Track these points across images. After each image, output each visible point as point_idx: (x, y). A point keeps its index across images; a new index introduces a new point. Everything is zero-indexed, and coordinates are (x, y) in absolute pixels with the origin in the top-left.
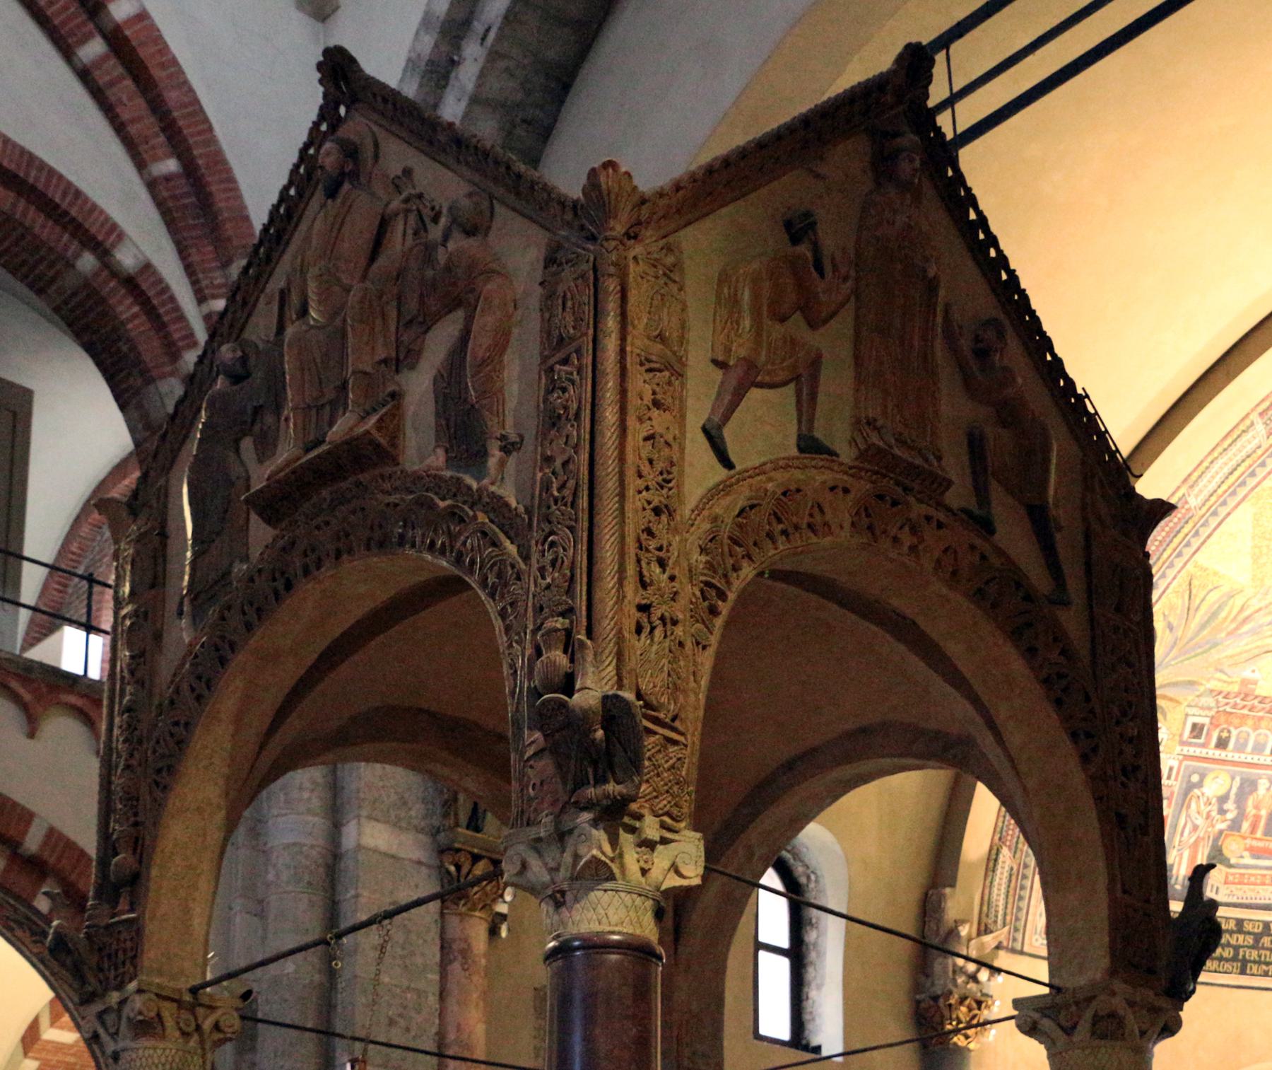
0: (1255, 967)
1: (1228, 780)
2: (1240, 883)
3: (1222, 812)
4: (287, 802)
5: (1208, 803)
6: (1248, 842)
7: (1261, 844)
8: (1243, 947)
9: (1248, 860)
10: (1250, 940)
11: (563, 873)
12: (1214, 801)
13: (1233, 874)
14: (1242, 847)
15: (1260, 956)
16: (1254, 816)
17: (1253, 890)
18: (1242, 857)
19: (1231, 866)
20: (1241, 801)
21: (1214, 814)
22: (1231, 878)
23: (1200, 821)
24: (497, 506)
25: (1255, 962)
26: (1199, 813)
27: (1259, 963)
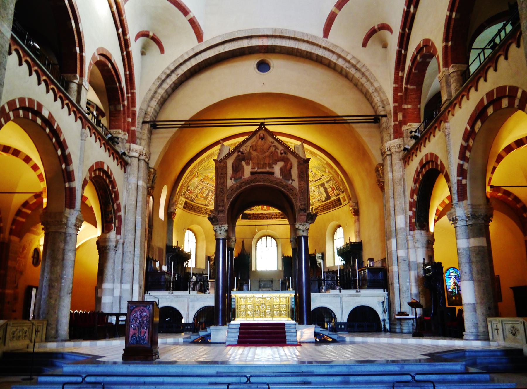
4: (134, 176)
9: (199, 197)
11: (304, 229)
23: (197, 191)
24: (293, 187)
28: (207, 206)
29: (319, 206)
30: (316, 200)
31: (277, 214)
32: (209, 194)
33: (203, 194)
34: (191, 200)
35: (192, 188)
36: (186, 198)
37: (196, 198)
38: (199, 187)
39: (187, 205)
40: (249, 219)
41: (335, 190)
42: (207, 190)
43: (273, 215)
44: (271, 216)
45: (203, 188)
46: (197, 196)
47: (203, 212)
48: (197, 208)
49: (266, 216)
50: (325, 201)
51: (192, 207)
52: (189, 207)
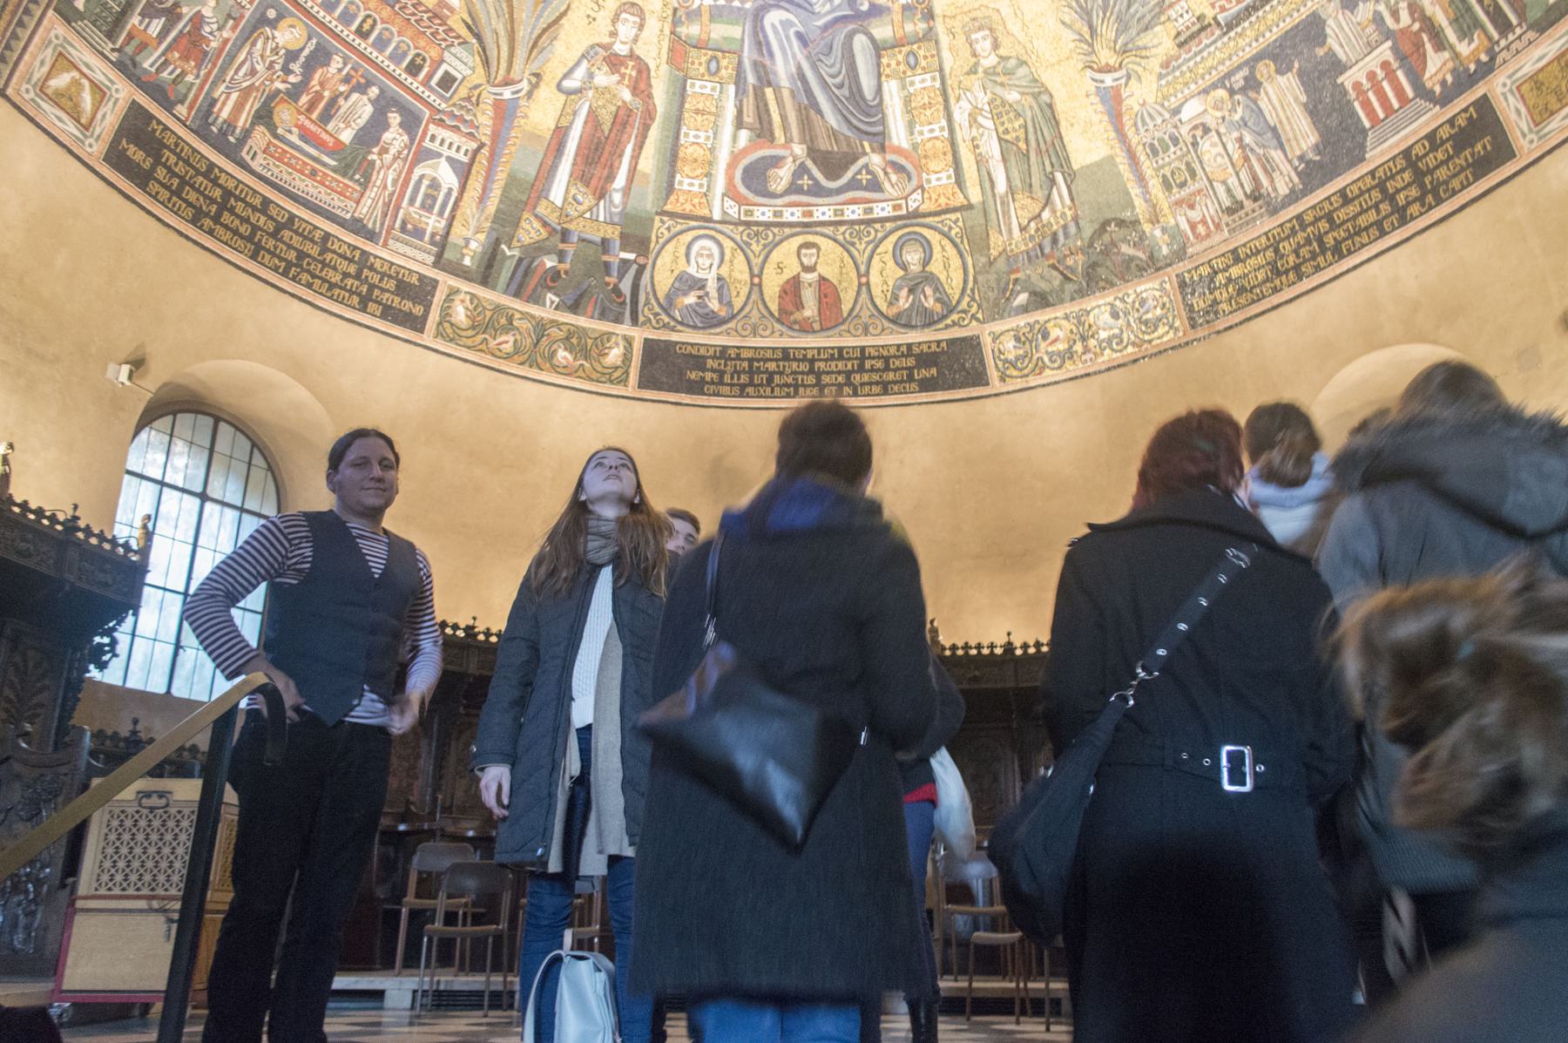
0: (268, 257)
1: (305, 35)
2: (278, 159)
3: (287, 70)
5: (275, 51)
6: (302, 118)
7: (313, 128)
8: (261, 229)
10: (271, 227)
12: (282, 52)
13: (275, 146)
14: (294, 122)
15: (276, 248)
16: (316, 92)
17: (290, 174)
18: (290, 132)
19: (276, 136)
20: (309, 69)
21: (278, 67)
22: (272, 149)
25: (268, 251)
26: (262, 56)
27: (273, 254)
28: (371, 236)
29: (1234, 251)
30: (1207, 209)
31: (886, 359)
32: (387, 136)
33: (326, 117)
34: (202, 132)
35: (207, 12)
36: (128, 68)
37: (260, 129)
38: (288, 35)
39: (158, 161)
40: (696, 388)
41: (1440, 44)
42: (362, 89)
43: (861, 369)
44: (848, 374)
45: (320, 57)
46: (264, 116)
47: (336, 278)
48: (279, 227)
49: (811, 371)
50: (1293, 197)
51: (223, 207)
52: (184, 182)
